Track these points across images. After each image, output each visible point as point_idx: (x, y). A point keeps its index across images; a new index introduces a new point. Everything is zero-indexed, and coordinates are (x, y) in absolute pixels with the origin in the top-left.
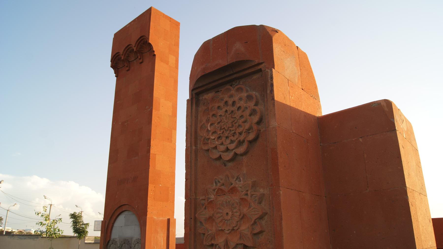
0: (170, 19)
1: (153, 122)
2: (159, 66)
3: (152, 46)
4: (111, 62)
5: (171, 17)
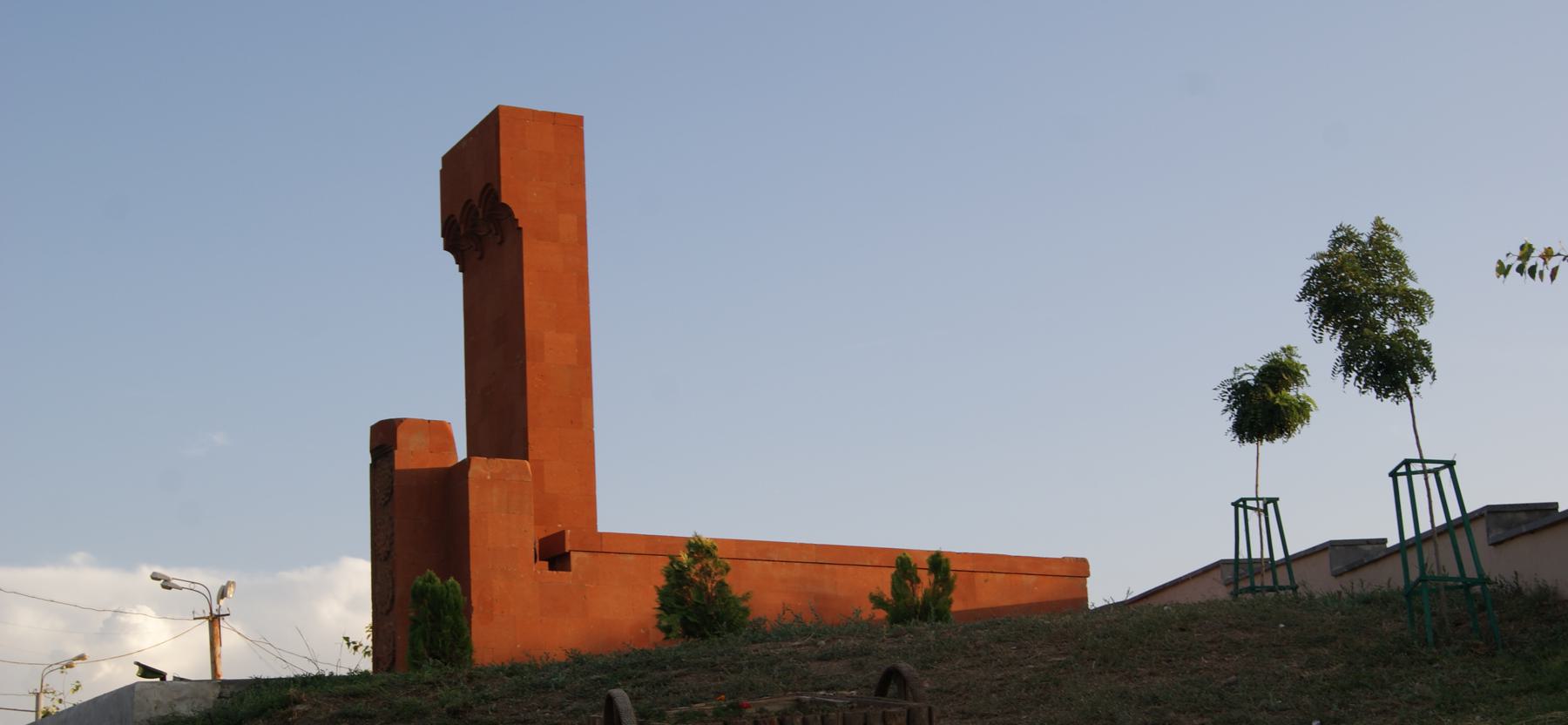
0: (554, 118)
1: (530, 391)
2: (536, 256)
3: (510, 208)
4: (442, 239)
5: (553, 111)
